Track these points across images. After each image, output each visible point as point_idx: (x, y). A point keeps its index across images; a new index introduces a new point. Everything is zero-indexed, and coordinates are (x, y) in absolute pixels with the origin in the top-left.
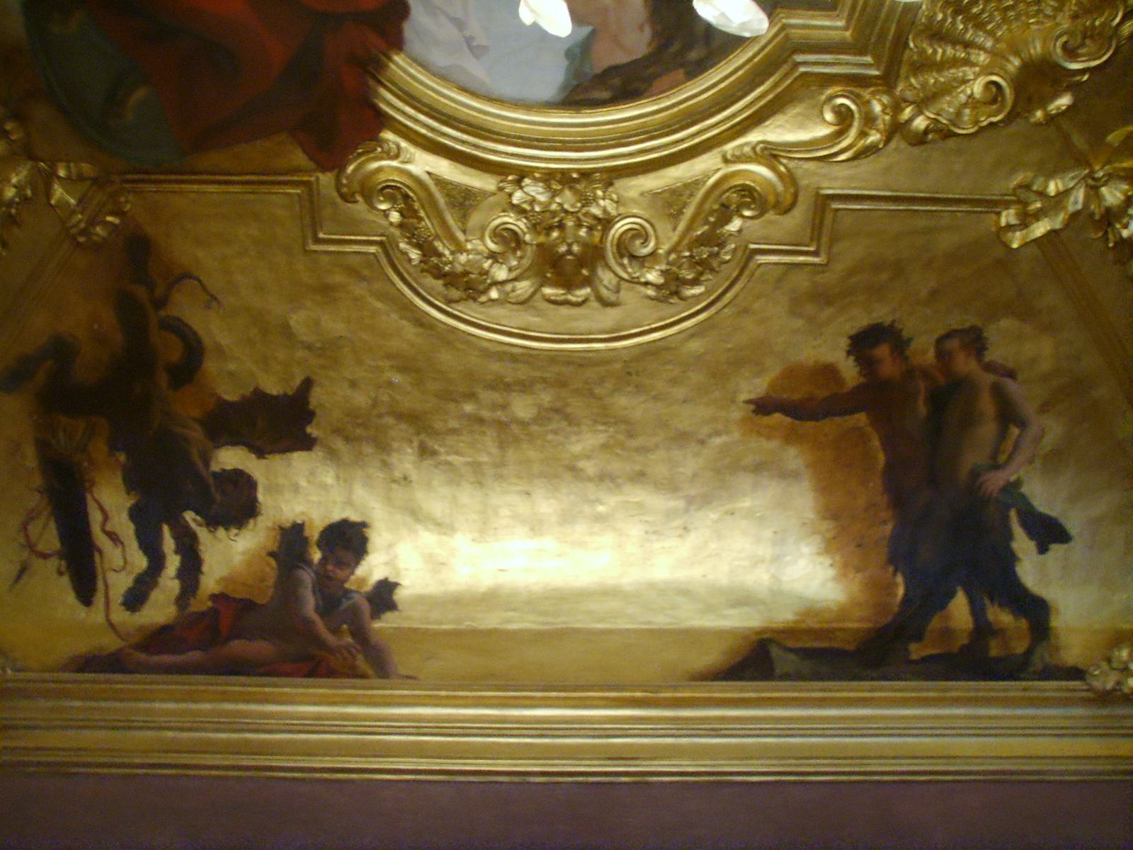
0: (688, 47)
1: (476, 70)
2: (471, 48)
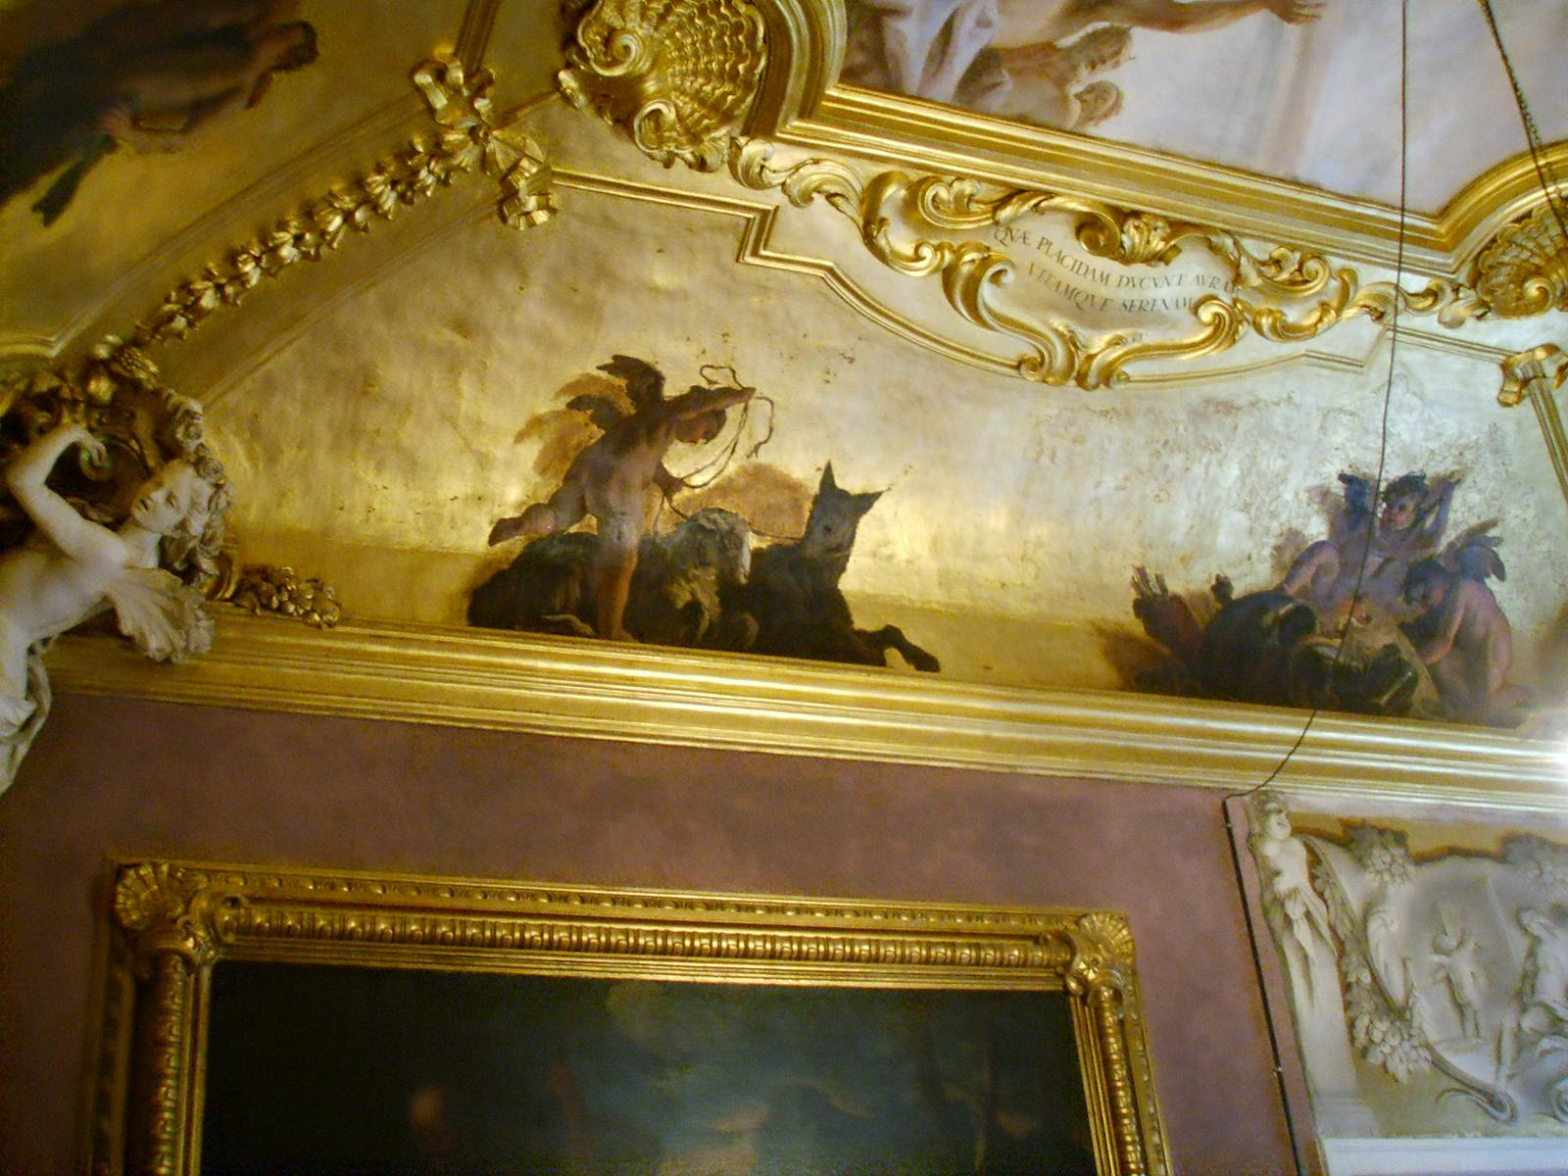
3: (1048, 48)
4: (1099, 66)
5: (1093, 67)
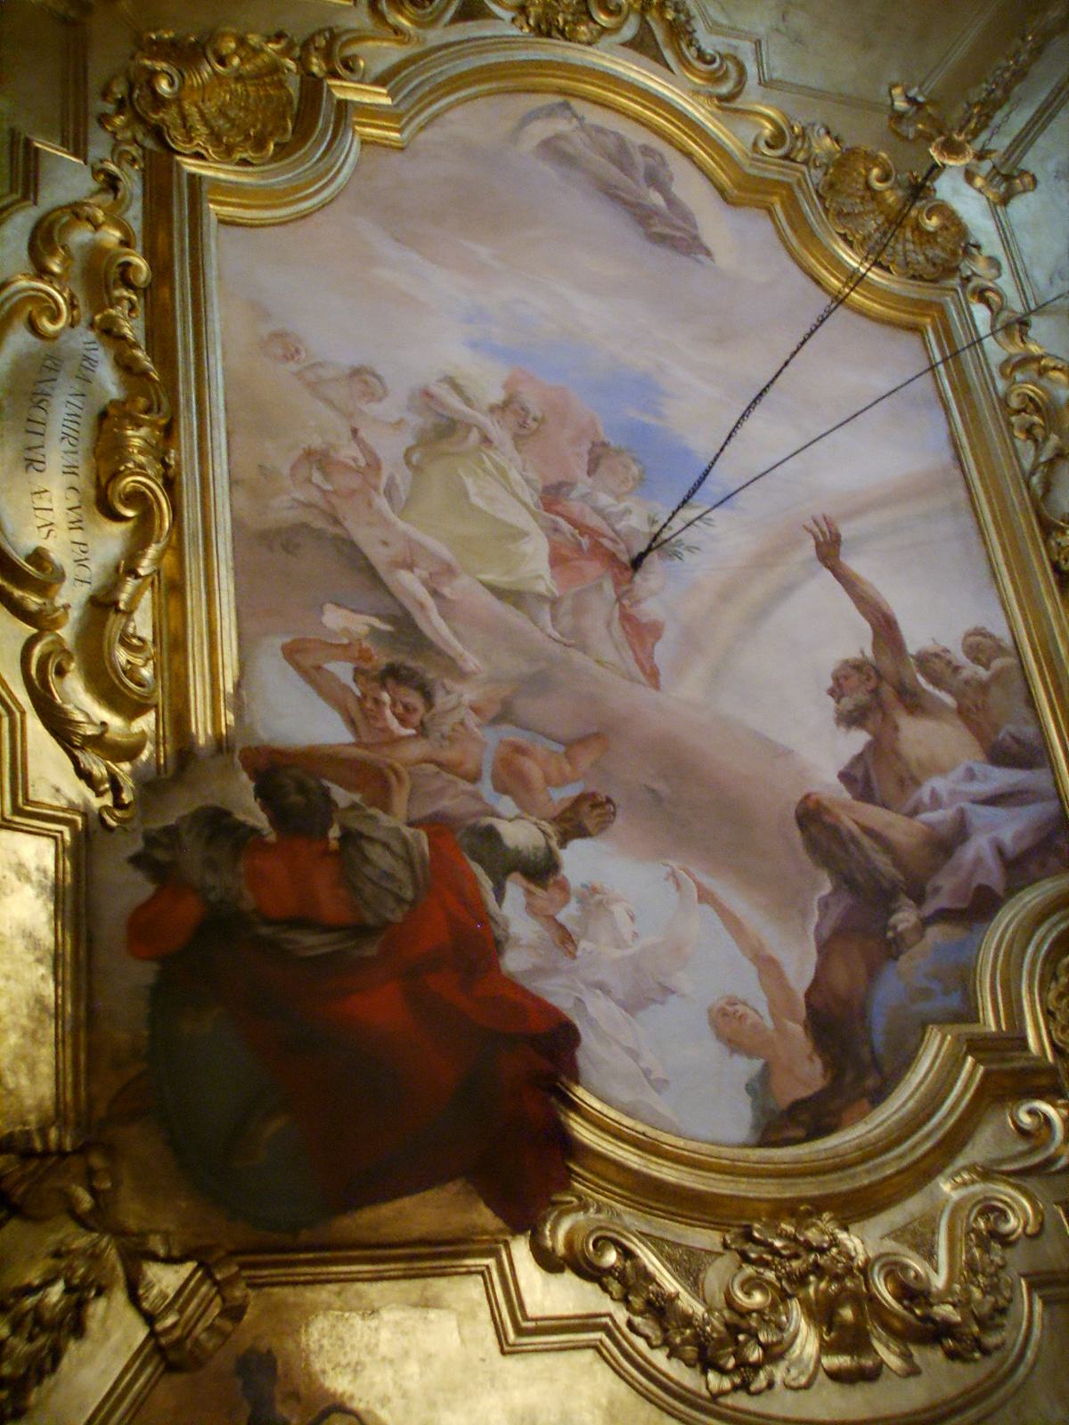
2: (649, 1081)
3: (961, 712)
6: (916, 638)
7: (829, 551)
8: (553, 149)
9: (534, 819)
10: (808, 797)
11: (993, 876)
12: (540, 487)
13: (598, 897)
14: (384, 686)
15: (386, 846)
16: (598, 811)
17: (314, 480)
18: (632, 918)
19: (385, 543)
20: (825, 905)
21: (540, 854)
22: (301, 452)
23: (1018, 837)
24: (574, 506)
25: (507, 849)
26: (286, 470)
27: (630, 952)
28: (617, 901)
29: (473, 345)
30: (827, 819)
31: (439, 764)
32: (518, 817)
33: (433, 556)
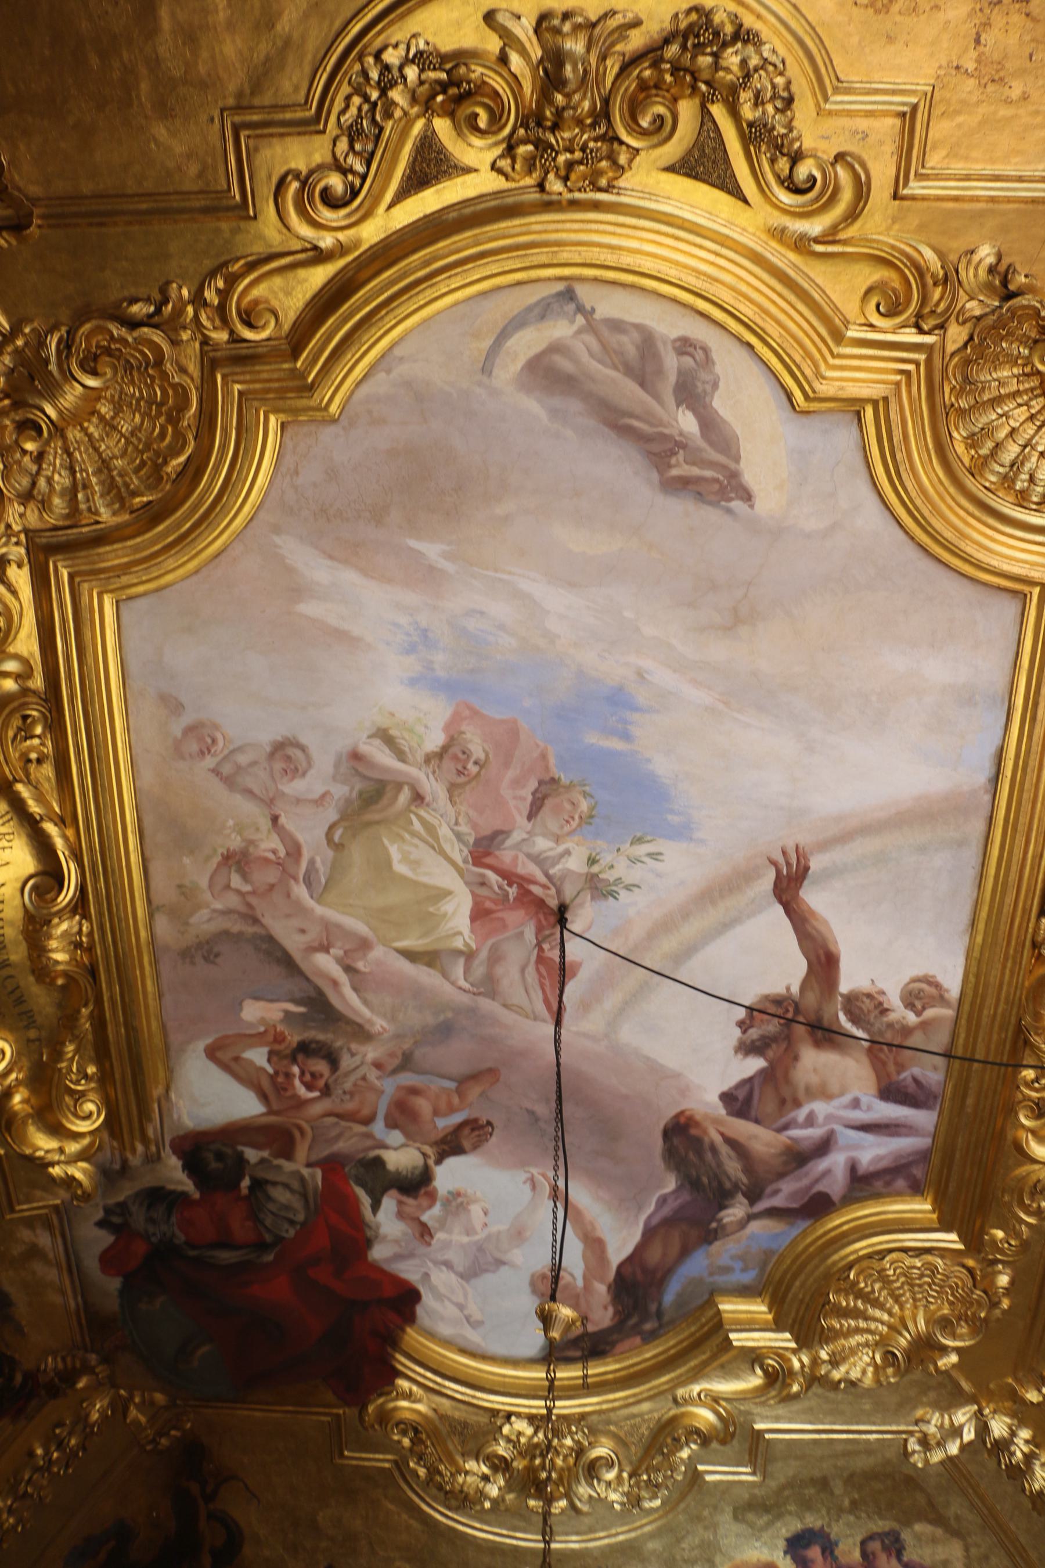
0: (643, 1320)
1: (474, 1337)
4: (885, 1006)
5: (887, 1010)
6: (851, 979)
7: (789, 885)
8: (547, 374)
9: (418, 1145)
10: (682, 1113)
11: (836, 1185)
12: (471, 840)
13: (460, 1200)
14: (294, 1060)
15: (286, 1186)
16: (477, 1133)
17: (233, 885)
18: (485, 1214)
19: (303, 931)
20: (663, 1200)
21: (417, 1172)
22: (220, 858)
23: (880, 1158)
24: (505, 856)
25: (388, 1172)
26: (204, 882)
27: (477, 1238)
28: (476, 1201)
29: (413, 682)
30: (693, 1131)
31: (338, 1116)
32: (403, 1146)
33: (348, 934)
